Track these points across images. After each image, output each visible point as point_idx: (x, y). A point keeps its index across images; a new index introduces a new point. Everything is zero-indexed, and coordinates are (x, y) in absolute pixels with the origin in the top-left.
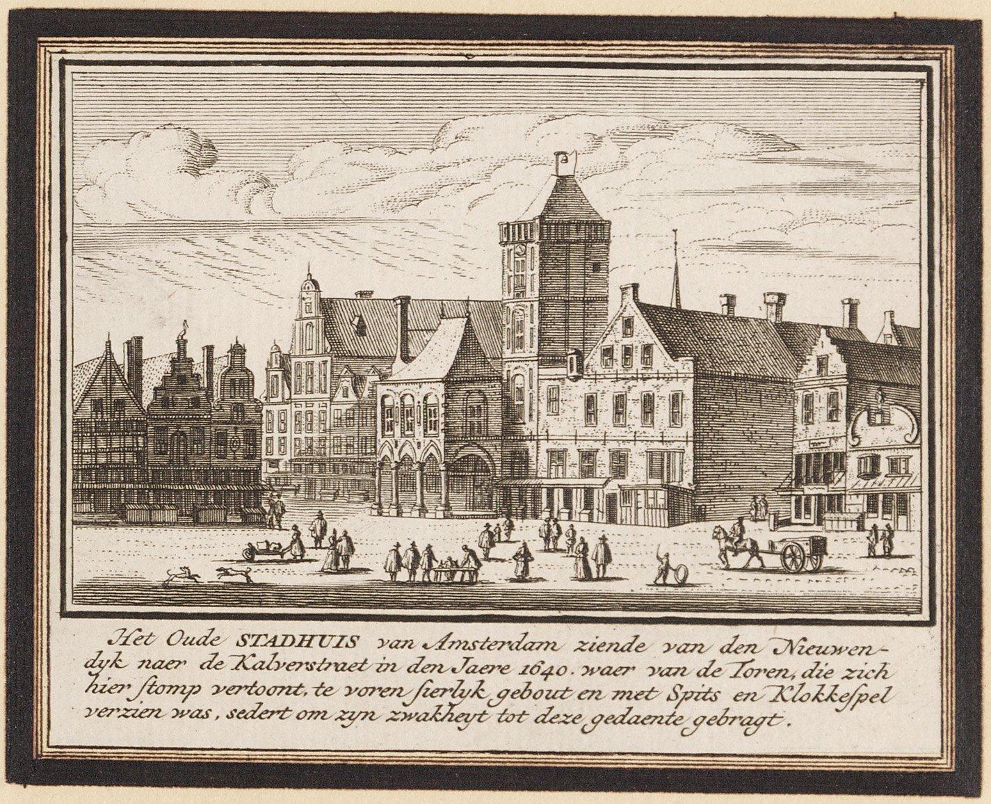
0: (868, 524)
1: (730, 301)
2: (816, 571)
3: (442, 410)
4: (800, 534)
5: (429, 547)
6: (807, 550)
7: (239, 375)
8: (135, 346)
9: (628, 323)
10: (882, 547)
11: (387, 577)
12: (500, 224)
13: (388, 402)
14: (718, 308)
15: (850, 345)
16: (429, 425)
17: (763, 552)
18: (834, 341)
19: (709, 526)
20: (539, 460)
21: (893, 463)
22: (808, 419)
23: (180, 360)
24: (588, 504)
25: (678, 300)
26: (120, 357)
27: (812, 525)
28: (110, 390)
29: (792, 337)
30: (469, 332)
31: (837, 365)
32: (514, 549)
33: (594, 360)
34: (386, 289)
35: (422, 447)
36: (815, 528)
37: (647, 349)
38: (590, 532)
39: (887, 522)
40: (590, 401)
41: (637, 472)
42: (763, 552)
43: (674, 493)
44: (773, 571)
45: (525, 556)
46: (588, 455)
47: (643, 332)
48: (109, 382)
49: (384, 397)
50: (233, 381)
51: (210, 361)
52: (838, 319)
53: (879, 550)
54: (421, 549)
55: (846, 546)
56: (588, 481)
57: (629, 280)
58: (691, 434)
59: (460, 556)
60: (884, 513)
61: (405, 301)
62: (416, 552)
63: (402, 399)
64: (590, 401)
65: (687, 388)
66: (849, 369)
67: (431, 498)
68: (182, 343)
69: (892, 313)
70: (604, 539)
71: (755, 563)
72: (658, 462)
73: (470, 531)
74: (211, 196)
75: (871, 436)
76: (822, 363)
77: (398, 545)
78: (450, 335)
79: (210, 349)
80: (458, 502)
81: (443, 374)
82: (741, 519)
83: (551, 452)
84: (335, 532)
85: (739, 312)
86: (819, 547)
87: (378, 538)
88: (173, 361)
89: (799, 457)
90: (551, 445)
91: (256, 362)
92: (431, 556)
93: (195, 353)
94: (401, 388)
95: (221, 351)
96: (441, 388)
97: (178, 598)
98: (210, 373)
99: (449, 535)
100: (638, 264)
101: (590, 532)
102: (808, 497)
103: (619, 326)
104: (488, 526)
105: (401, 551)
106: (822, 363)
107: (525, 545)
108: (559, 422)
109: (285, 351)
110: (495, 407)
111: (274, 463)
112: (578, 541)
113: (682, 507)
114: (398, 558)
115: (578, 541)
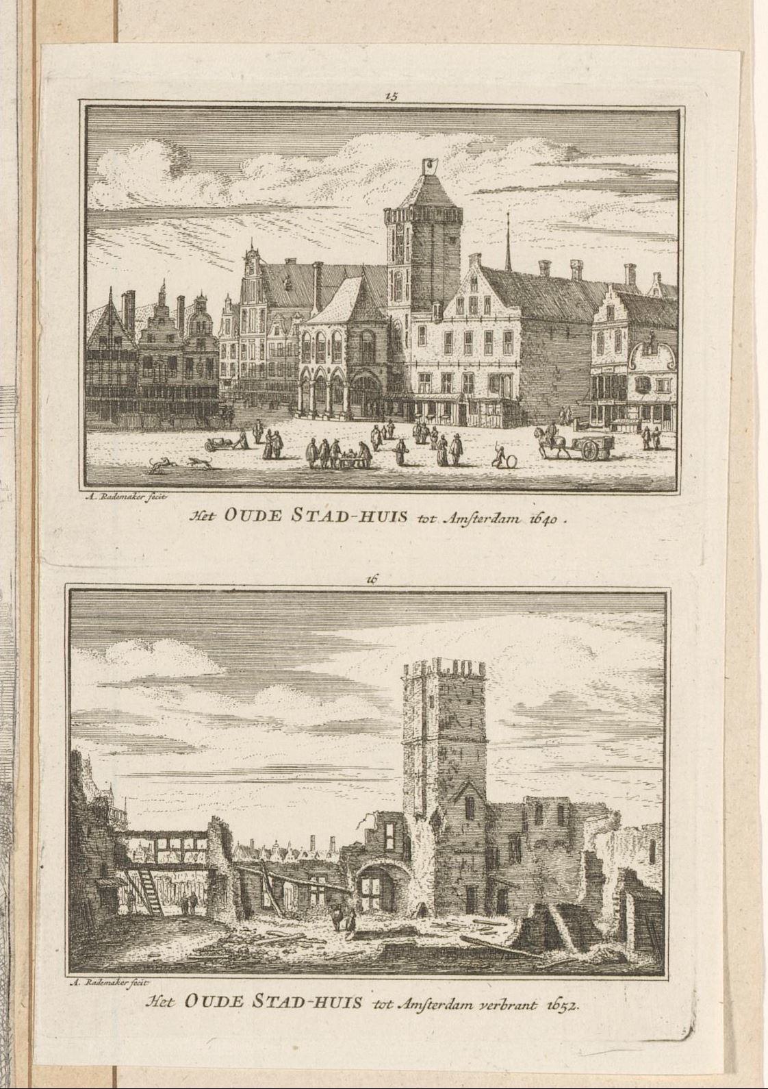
0: (643, 427)
1: (545, 265)
2: (606, 459)
3: (344, 344)
4: (598, 432)
5: (337, 441)
6: (601, 446)
7: (201, 318)
8: (130, 296)
9: (474, 281)
10: (652, 442)
11: (308, 464)
12: (385, 211)
13: (307, 337)
14: (536, 272)
15: (630, 299)
16: (335, 357)
17: (568, 448)
18: (619, 295)
19: (532, 429)
20: (414, 381)
21: (660, 382)
22: (600, 351)
23: (161, 306)
24: (448, 411)
25: (509, 267)
26: (119, 304)
27: (602, 427)
28: (111, 331)
29: (588, 294)
30: (363, 288)
31: (621, 314)
32: (394, 444)
33: (451, 310)
34: (306, 257)
35: (331, 372)
36: (604, 429)
37: (488, 300)
38: (448, 431)
39: (656, 425)
40: (449, 336)
41: (481, 389)
42: (568, 448)
43: (506, 403)
44: (579, 459)
45: (401, 450)
46: (447, 377)
47: (485, 288)
48: (111, 323)
49: (305, 333)
50: (198, 323)
51: (181, 308)
52: (621, 277)
53: (652, 444)
54: (331, 442)
55: (628, 442)
56: (447, 396)
57: (475, 250)
58: (519, 360)
59: (357, 449)
60: (654, 418)
61: (319, 265)
62: (328, 445)
63: (317, 336)
64: (449, 336)
65: (517, 327)
66: (630, 315)
67: (336, 408)
68: (162, 295)
69: (659, 276)
70: (457, 437)
71: (563, 453)
72: (495, 381)
73: (363, 431)
74: (185, 191)
75: (644, 364)
76: (611, 310)
77: (313, 441)
78: (350, 289)
79: (181, 299)
80: (357, 409)
81: (346, 319)
82: (553, 424)
83: (422, 375)
84: (269, 432)
85: (554, 272)
86: (609, 444)
87: (299, 435)
88: (156, 309)
89: (594, 378)
90: (420, 369)
91: (215, 310)
92: (338, 450)
93: (172, 304)
94: (316, 328)
95: (189, 302)
96: (344, 329)
97: (161, 477)
98: (182, 319)
99: (352, 434)
100: (480, 240)
101: (448, 431)
102: (600, 407)
103: (469, 285)
104: (376, 428)
105: (318, 445)
106: (611, 310)
107: (402, 441)
108: (425, 355)
109: (236, 300)
110: (381, 344)
111: (227, 383)
112: (440, 438)
113: (514, 415)
114: (316, 452)
115: (440, 438)
